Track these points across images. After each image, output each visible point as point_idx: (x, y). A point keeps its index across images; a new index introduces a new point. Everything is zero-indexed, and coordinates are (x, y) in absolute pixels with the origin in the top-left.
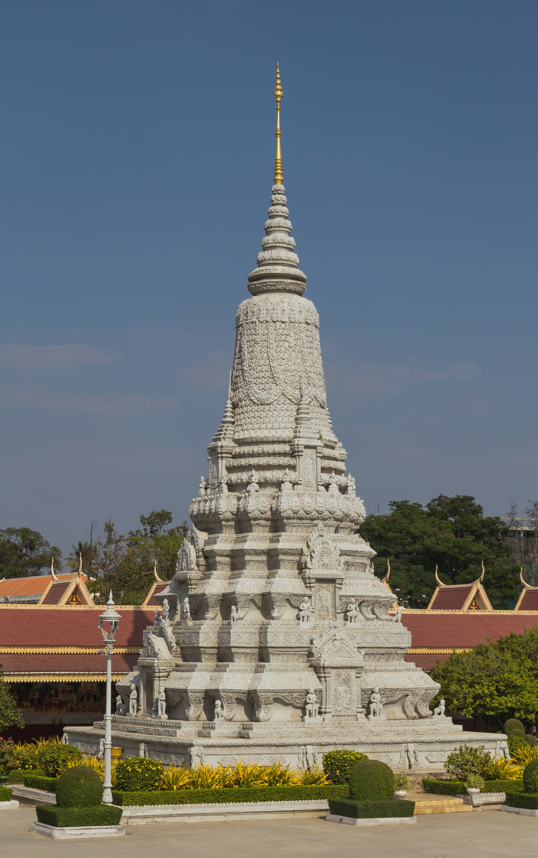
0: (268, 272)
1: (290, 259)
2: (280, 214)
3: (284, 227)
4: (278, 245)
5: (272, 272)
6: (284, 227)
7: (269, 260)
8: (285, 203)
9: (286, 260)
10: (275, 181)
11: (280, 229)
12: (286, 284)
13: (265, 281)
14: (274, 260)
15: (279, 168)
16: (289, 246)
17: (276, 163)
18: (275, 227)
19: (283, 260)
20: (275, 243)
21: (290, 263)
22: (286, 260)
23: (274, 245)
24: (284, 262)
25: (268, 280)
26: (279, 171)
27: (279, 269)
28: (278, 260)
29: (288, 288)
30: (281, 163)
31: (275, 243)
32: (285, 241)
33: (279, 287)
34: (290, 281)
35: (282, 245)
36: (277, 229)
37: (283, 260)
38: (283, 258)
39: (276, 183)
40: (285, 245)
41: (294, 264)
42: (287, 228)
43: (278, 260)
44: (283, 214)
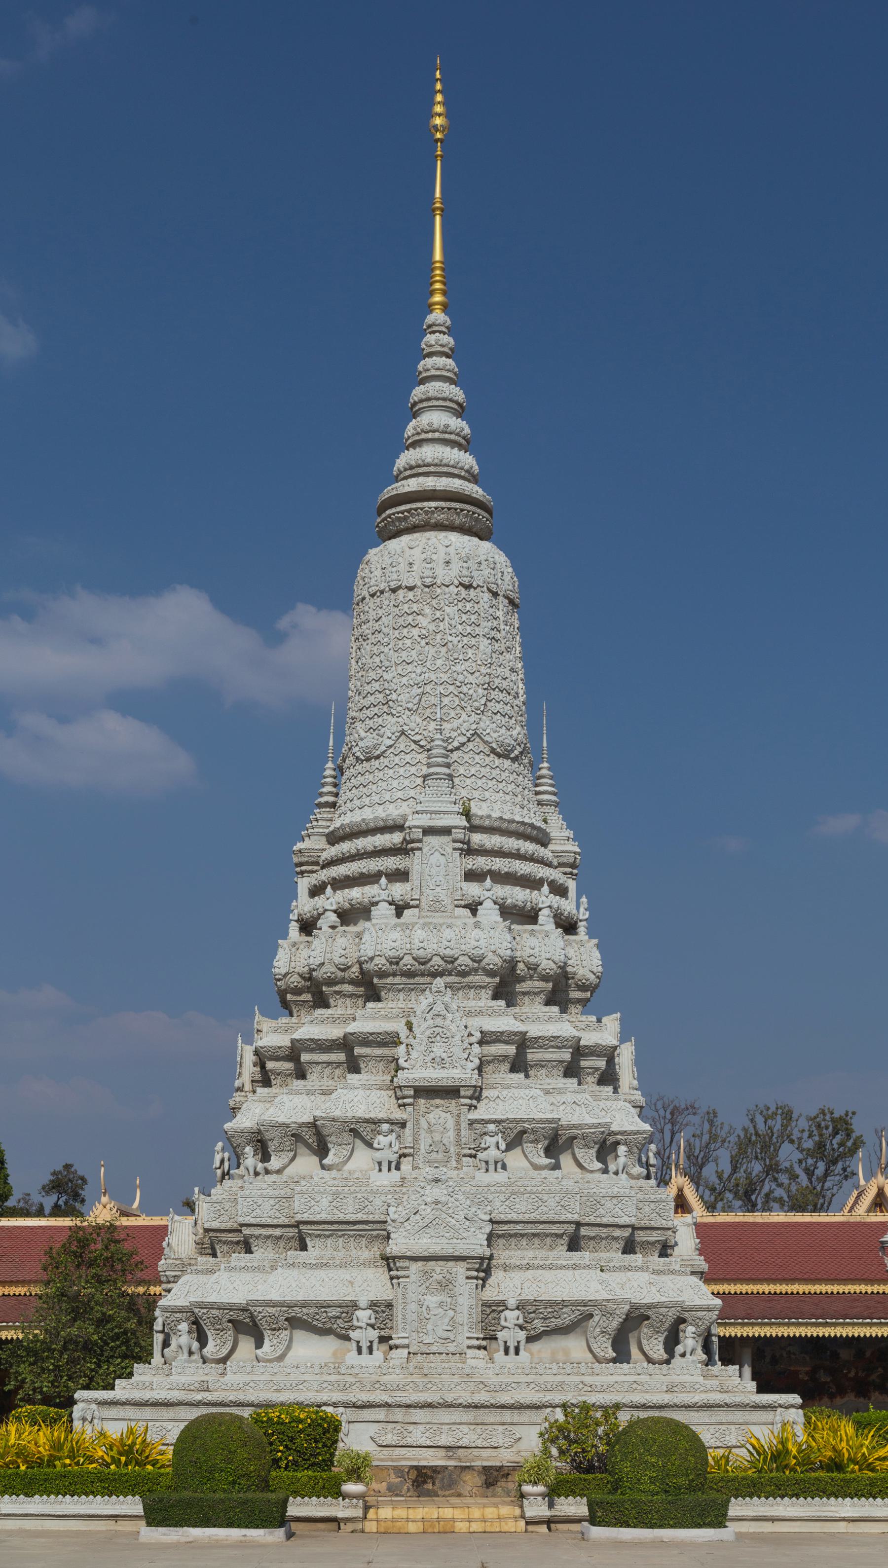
0: (395, 492)
1: (444, 461)
2: (433, 372)
3: (438, 399)
4: (423, 436)
5: (407, 489)
6: (438, 399)
7: (406, 470)
8: (446, 350)
9: (436, 465)
10: (430, 309)
11: (430, 404)
12: (426, 513)
13: (388, 512)
14: (411, 468)
15: (438, 278)
16: (447, 436)
17: (433, 270)
18: (421, 401)
19: (428, 465)
20: (418, 434)
21: (445, 469)
22: (436, 465)
23: (417, 438)
24: (432, 469)
25: (393, 510)
26: (438, 286)
27: (412, 485)
28: (419, 466)
29: (433, 521)
30: (443, 269)
31: (418, 434)
32: (435, 426)
33: (414, 520)
34: (433, 504)
35: (430, 436)
36: (425, 404)
37: (428, 465)
38: (429, 460)
39: (431, 312)
40: (437, 435)
41: (456, 471)
42: (444, 399)
43: (419, 466)
44: (438, 373)
